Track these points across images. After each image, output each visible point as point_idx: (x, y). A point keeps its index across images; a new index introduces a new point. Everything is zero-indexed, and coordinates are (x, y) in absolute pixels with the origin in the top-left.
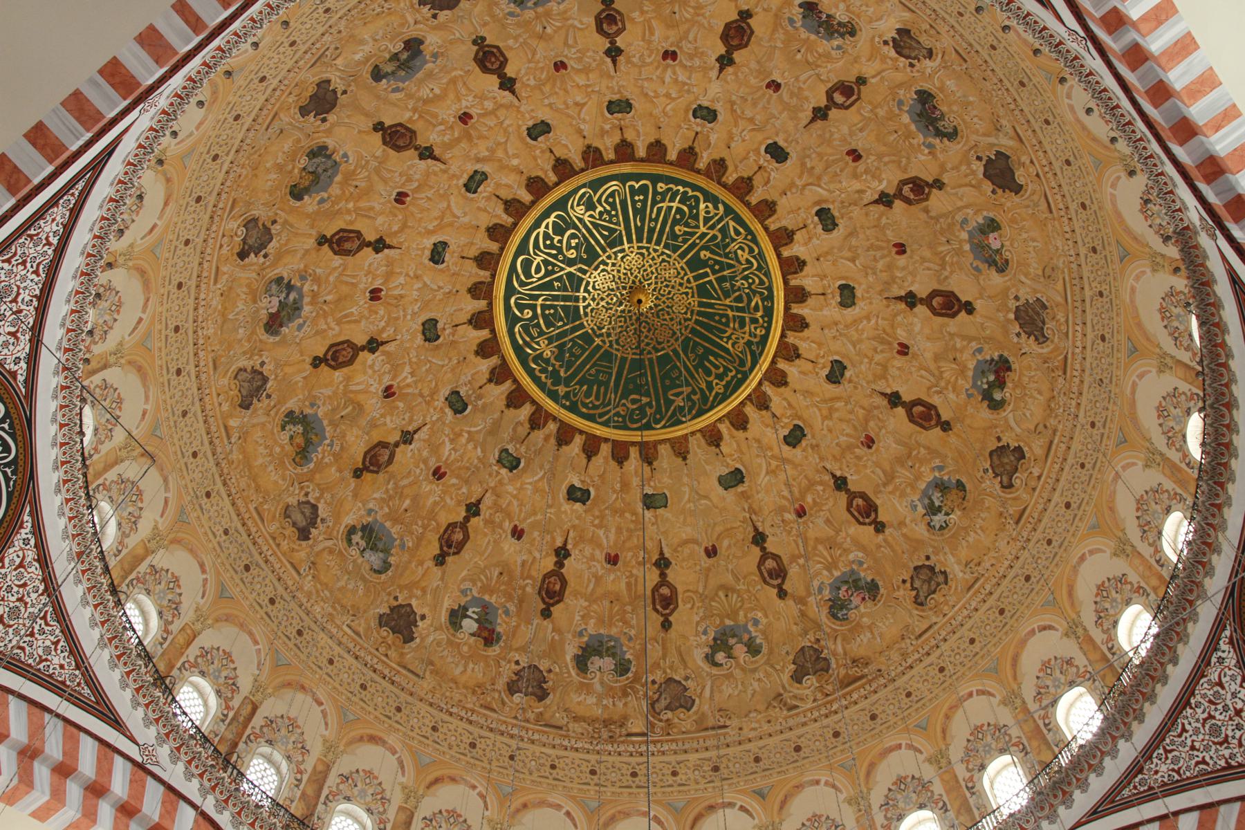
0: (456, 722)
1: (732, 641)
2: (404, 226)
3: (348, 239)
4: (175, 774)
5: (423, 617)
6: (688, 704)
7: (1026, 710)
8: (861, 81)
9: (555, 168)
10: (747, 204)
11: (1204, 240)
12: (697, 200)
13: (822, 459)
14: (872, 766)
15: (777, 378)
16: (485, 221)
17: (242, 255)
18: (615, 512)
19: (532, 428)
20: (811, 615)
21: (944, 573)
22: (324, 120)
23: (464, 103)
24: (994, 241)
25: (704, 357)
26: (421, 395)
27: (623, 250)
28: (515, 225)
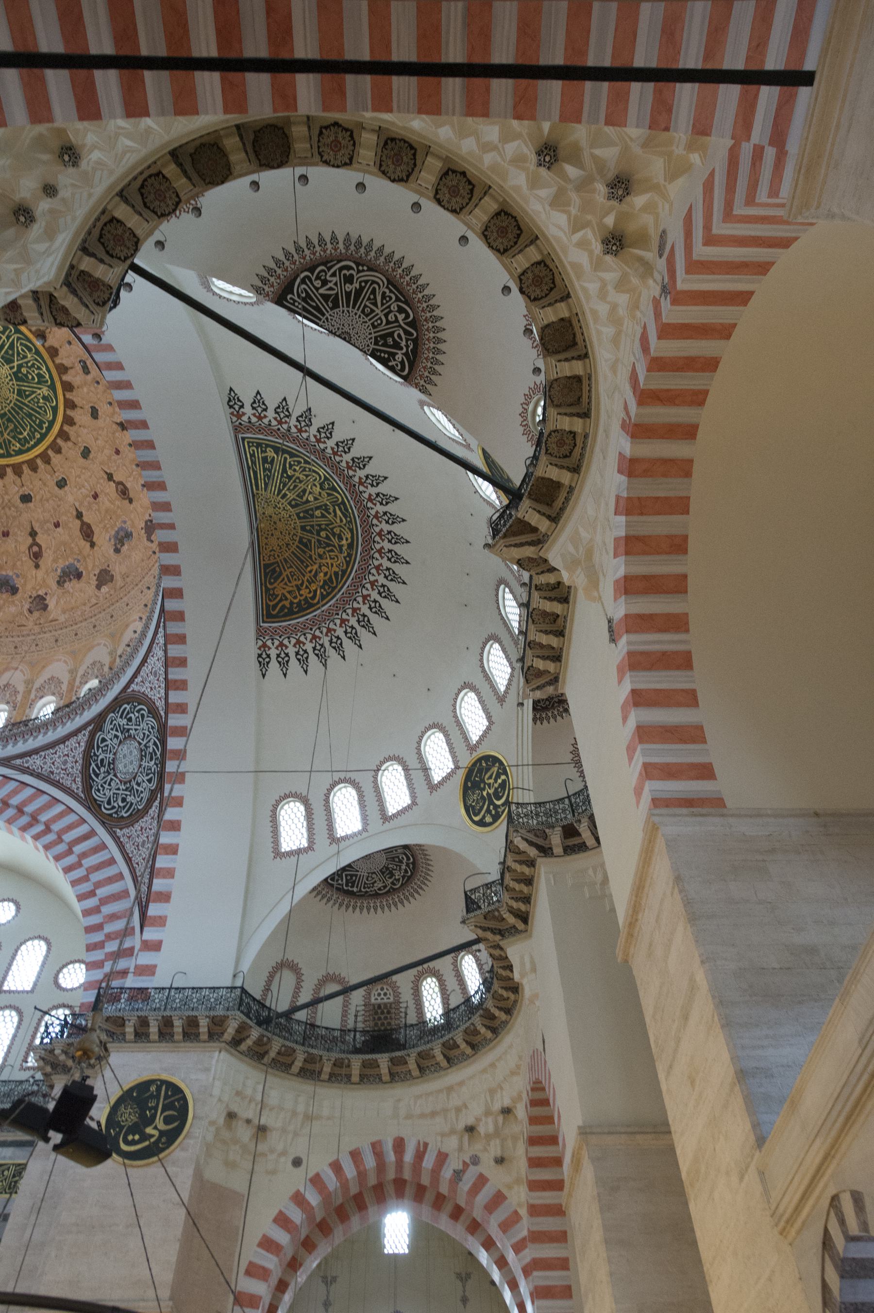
8: (37, 566)
12: (23, 445)
16: (62, 352)
27: (14, 393)
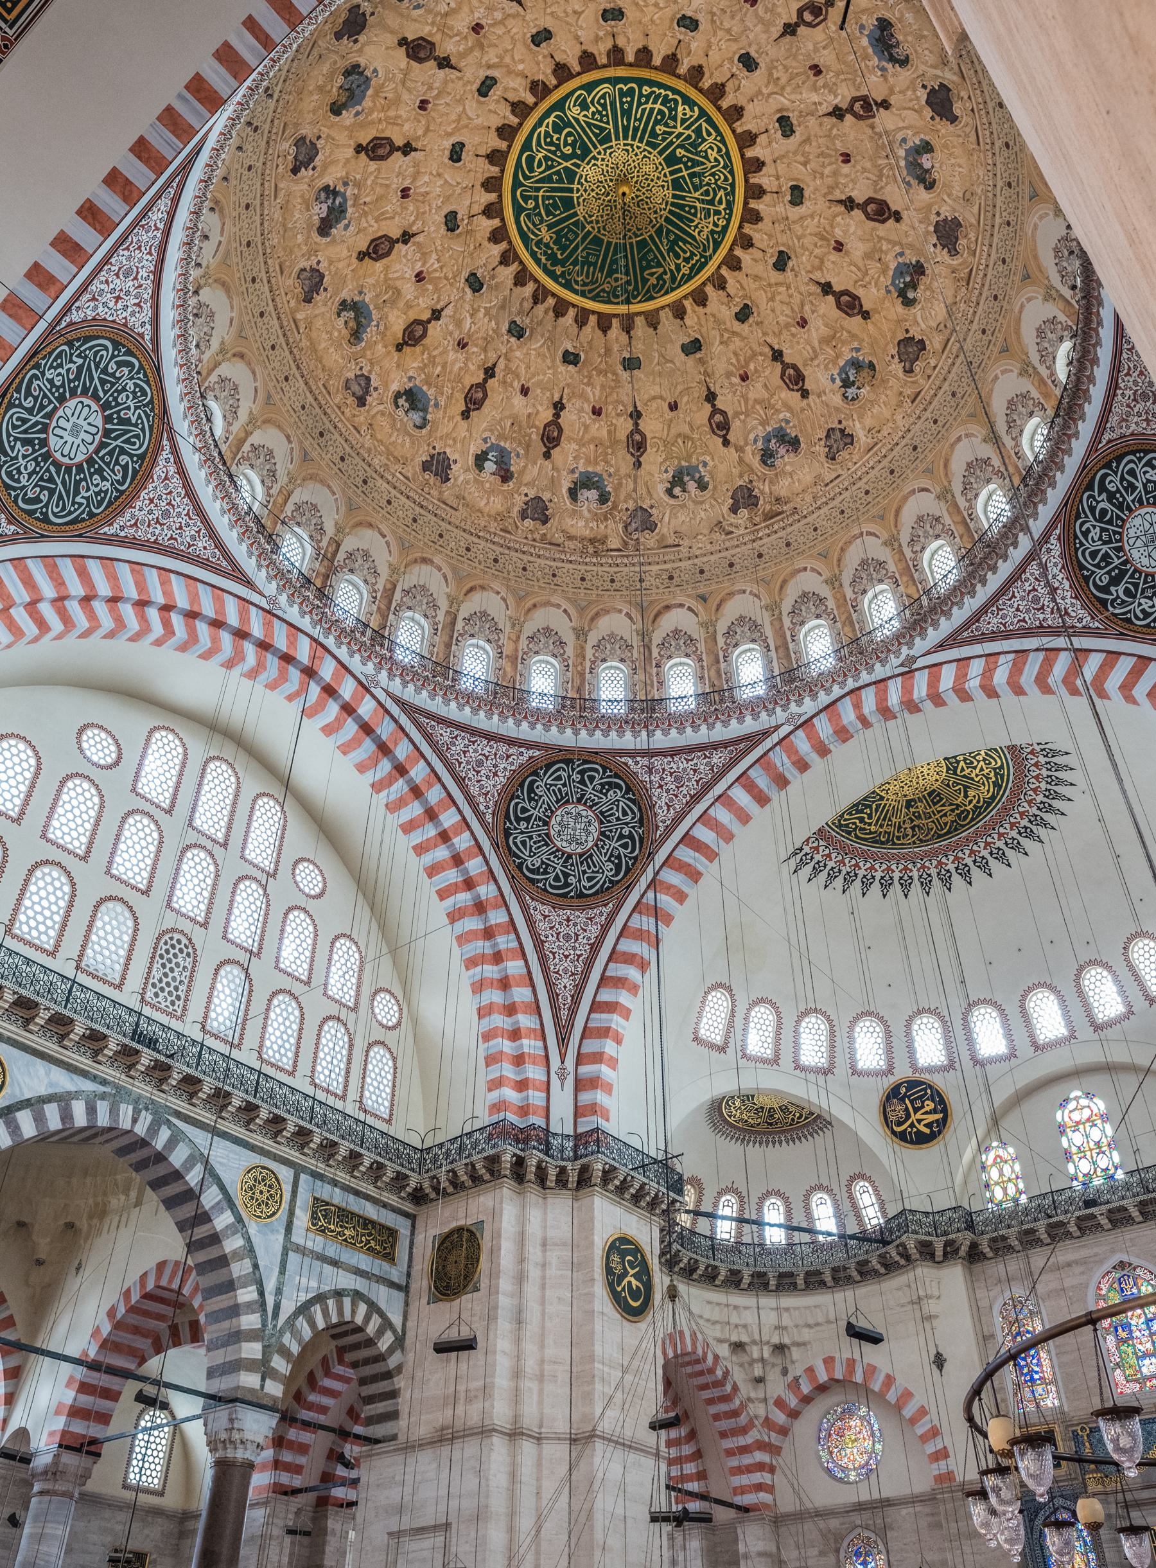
0: (483, 543)
2: (427, 130)
3: (381, 146)
4: (292, 613)
5: (455, 462)
6: (652, 527)
7: (902, 553)
9: (555, 72)
10: (719, 108)
13: (765, 334)
14: (785, 582)
15: (734, 264)
16: (496, 122)
17: (295, 171)
18: (600, 372)
19: (535, 303)
20: (747, 460)
22: (356, 41)
23: (477, 15)
24: (926, 161)
25: (674, 243)
26: (446, 278)
28: (521, 124)
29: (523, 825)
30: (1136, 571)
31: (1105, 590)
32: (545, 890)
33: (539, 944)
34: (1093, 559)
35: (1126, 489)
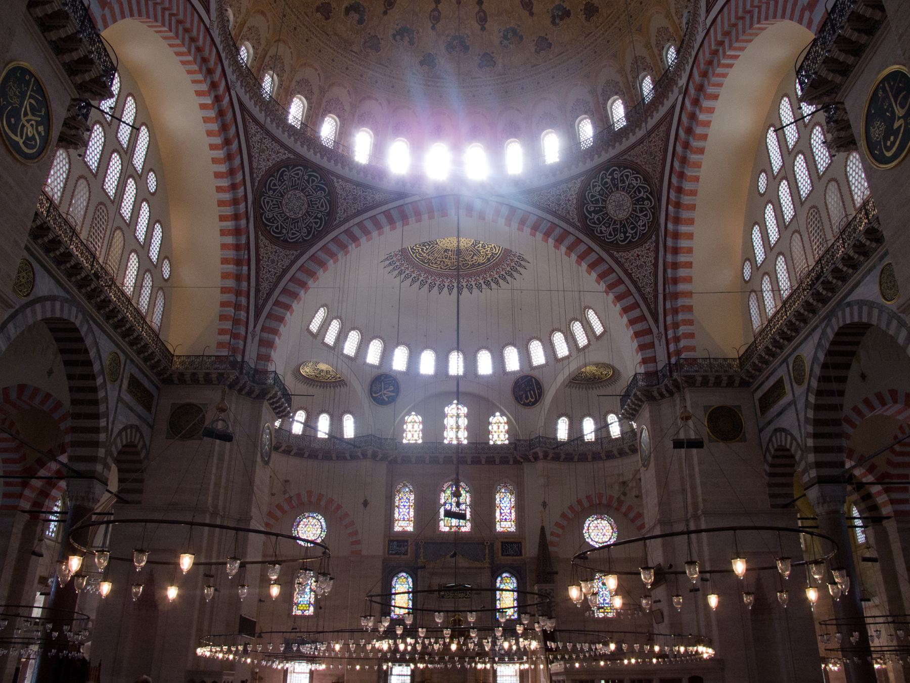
1: (405, 34)
11: (676, 90)
21: (495, 63)
29: (271, 193)
30: (606, 213)
31: (590, 213)
32: (270, 232)
33: (258, 261)
34: (592, 198)
35: (621, 181)
